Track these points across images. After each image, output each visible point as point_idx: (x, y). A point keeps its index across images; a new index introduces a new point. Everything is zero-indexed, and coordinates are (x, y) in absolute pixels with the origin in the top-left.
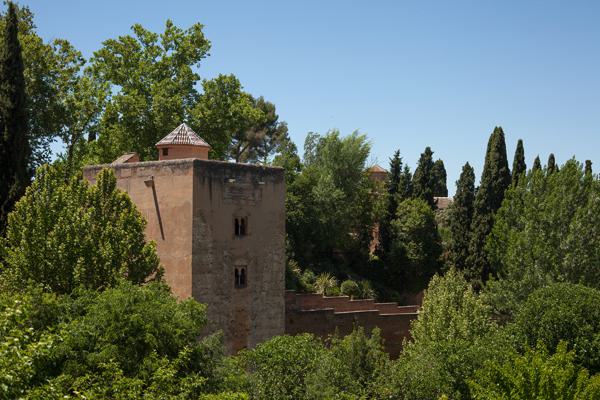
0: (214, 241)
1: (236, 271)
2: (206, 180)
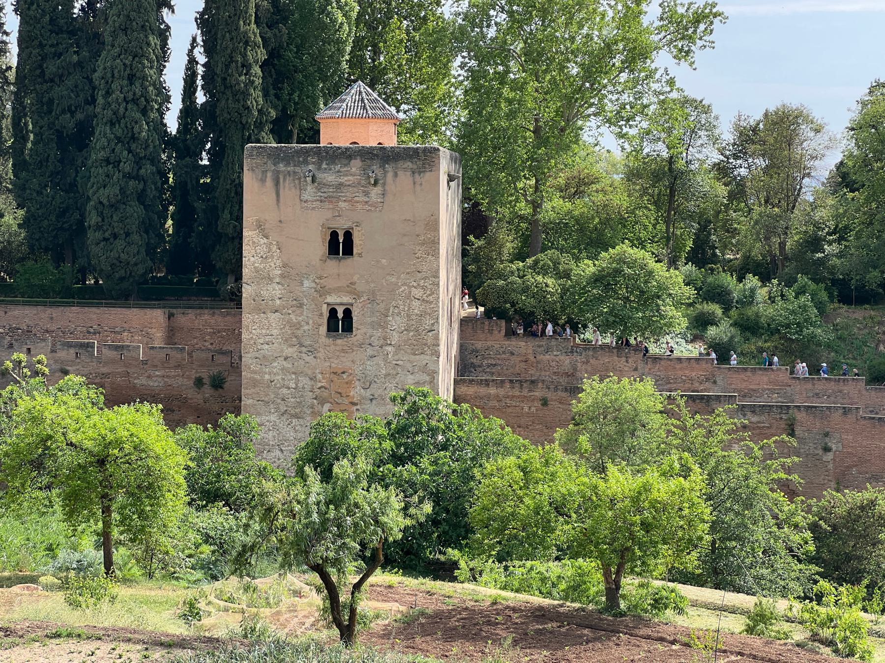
0: (285, 266)
1: (333, 312)
2: (269, 174)
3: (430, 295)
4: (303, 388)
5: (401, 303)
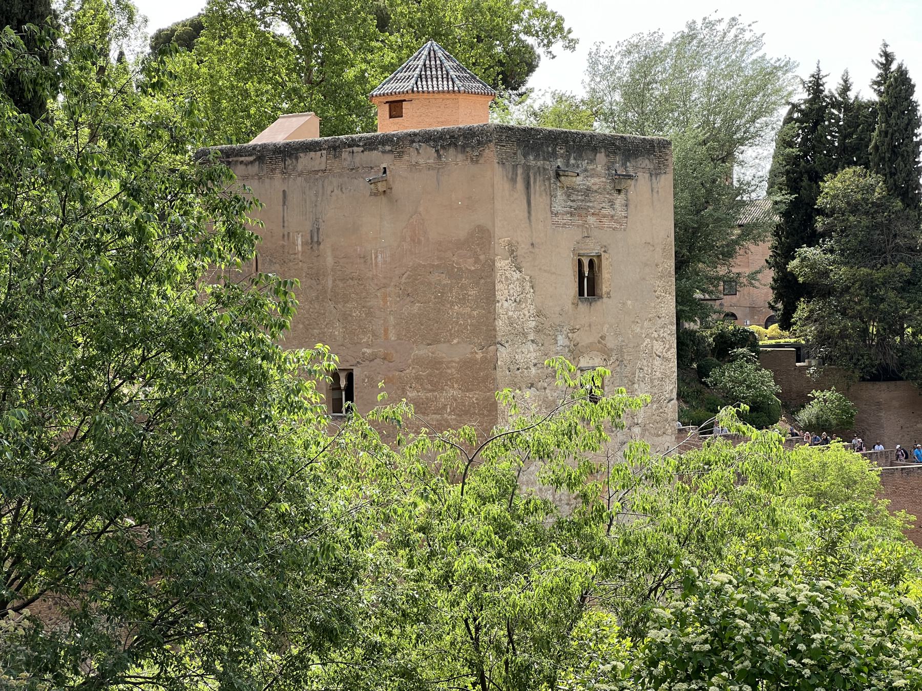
0: (539, 314)
2: (520, 171)
3: (668, 350)
4: (560, 500)
5: (645, 363)
